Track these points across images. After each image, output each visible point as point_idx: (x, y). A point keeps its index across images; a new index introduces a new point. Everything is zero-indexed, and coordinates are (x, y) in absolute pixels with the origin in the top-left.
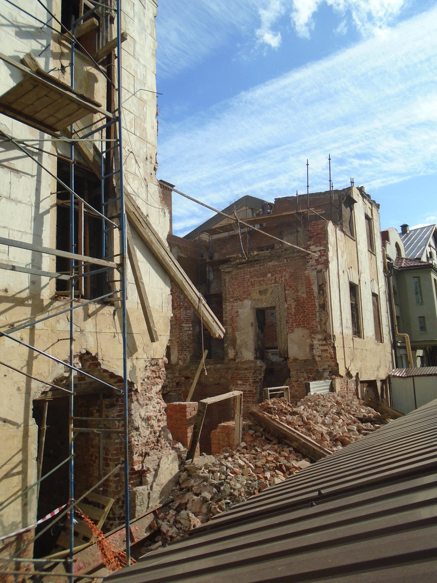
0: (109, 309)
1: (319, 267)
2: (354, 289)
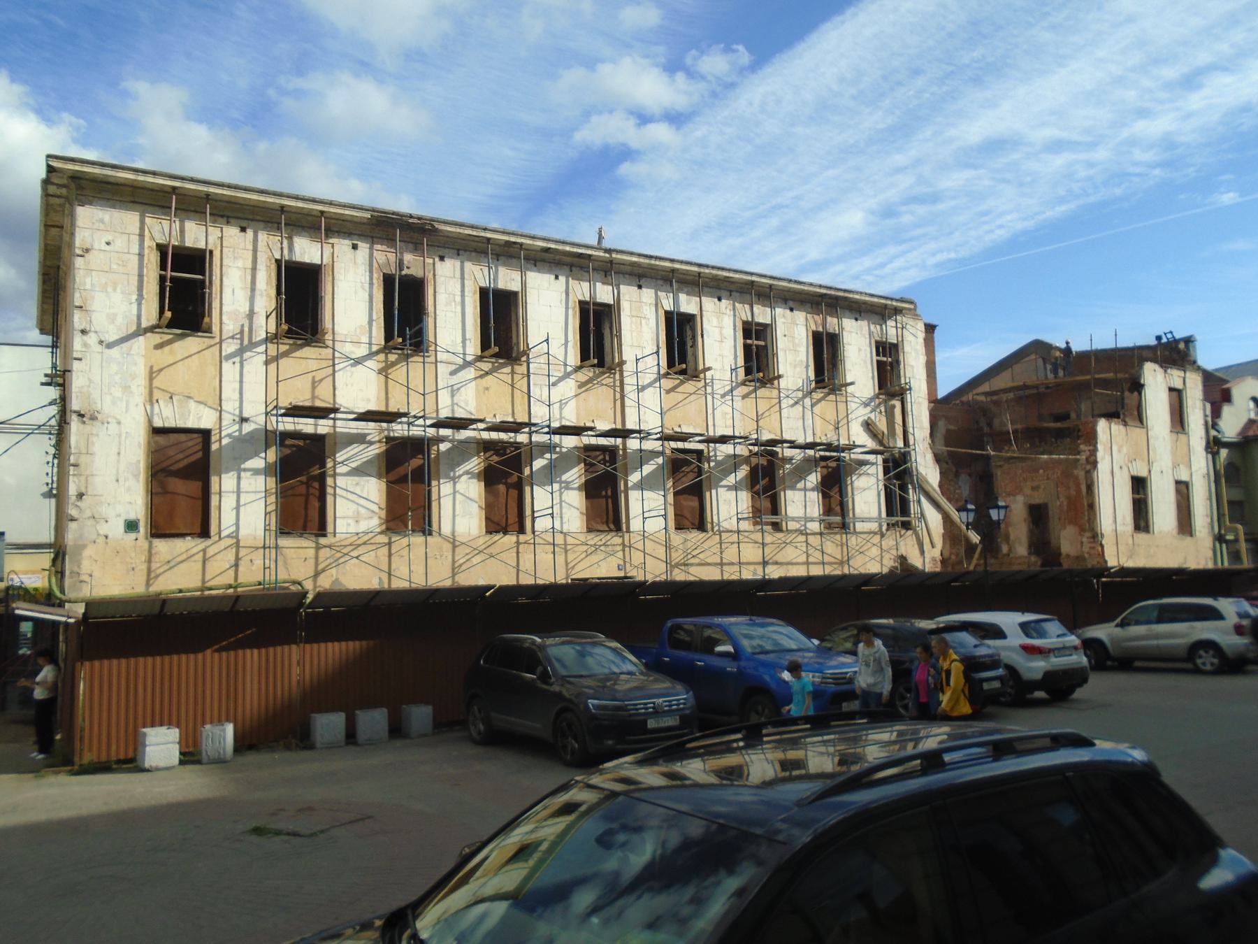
0: (910, 532)
1: (1088, 467)
2: (1139, 484)
